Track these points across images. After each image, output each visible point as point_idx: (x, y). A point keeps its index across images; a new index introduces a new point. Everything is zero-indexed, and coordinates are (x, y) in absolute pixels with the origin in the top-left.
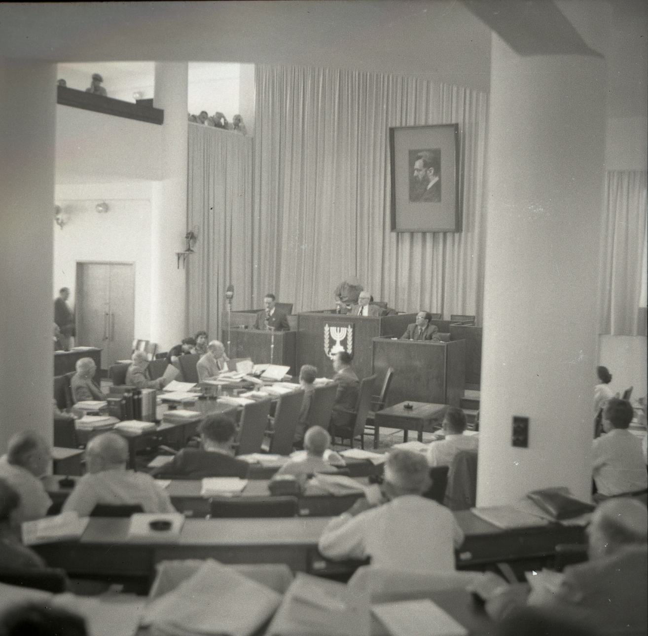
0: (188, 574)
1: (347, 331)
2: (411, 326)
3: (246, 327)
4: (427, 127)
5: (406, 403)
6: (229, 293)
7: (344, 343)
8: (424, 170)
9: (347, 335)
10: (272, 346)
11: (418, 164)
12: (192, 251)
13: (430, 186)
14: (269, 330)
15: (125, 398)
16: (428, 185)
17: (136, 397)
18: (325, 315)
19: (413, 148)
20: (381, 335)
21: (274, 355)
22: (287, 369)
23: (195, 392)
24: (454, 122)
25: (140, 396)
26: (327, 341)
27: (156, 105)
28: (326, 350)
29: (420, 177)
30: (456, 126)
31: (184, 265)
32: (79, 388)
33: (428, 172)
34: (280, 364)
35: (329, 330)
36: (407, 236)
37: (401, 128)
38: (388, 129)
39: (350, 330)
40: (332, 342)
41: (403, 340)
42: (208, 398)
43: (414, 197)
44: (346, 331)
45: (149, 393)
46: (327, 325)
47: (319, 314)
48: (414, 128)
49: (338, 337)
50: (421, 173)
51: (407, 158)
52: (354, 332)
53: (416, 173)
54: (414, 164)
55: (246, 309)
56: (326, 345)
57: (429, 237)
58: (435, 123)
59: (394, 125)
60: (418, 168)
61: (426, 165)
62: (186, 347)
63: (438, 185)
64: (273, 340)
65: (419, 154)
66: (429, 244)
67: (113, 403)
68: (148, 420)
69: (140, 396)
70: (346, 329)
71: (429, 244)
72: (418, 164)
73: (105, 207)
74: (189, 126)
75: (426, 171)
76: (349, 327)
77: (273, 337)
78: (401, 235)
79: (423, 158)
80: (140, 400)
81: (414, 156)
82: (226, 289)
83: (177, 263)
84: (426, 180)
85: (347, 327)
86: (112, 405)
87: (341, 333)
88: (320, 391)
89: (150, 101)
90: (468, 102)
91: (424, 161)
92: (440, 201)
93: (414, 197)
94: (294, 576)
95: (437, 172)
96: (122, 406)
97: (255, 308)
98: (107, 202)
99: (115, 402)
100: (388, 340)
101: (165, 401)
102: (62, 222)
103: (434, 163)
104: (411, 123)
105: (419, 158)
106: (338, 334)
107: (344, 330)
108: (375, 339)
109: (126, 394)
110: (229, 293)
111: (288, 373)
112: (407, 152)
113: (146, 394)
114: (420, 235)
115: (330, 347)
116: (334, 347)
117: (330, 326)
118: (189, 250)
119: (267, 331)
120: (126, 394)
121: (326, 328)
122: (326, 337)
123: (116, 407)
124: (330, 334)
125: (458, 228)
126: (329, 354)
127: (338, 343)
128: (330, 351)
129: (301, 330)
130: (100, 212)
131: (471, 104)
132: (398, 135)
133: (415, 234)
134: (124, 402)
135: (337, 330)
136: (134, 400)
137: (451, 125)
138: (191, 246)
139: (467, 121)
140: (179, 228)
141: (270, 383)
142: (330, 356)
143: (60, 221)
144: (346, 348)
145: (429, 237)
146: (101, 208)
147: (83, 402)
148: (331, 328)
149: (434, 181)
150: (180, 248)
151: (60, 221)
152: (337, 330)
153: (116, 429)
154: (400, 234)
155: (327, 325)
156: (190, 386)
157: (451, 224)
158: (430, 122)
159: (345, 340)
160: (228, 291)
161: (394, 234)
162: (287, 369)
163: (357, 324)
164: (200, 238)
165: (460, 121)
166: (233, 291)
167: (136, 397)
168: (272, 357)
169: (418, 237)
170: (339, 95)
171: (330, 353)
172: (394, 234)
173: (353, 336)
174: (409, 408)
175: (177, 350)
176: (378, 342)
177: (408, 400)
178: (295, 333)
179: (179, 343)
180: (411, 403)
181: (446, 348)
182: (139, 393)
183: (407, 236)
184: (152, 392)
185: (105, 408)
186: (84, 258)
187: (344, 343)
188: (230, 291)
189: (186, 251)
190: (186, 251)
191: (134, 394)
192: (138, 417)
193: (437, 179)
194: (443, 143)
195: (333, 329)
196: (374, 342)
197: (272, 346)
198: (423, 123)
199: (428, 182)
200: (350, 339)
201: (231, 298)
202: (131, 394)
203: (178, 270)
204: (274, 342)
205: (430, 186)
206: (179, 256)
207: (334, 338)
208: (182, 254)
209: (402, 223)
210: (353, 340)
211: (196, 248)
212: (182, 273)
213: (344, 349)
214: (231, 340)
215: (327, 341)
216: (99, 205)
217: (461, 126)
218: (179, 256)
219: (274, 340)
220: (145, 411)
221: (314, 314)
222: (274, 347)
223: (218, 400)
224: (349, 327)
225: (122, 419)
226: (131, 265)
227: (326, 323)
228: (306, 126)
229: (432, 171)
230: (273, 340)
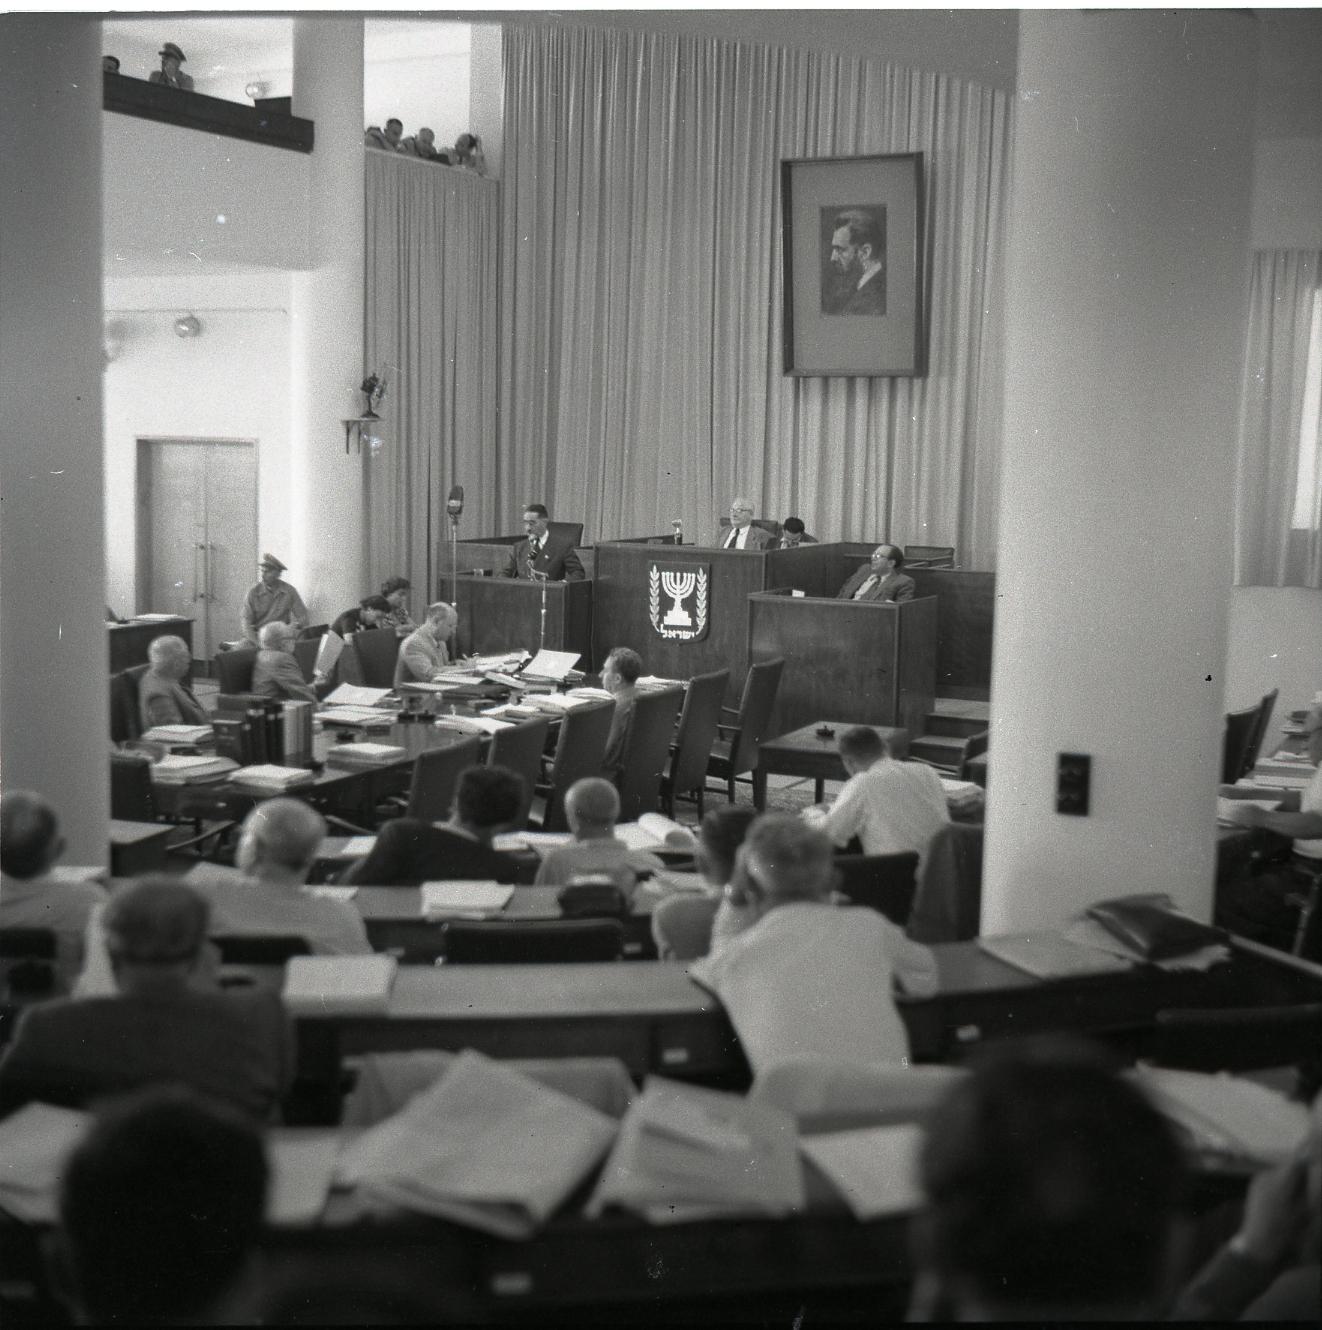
0: (423, 1083)
1: (697, 580)
3: (488, 573)
4: (858, 159)
5: (821, 725)
6: (454, 503)
7: (689, 604)
8: (851, 249)
9: (696, 588)
10: (543, 611)
11: (840, 236)
12: (376, 416)
13: (862, 282)
14: (536, 578)
15: (250, 719)
16: (859, 278)
17: (271, 717)
18: (650, 546)
19: (827, 203)
20: (765, 589)
21: (545, 631)
22: (575, 657)
23: (390, 706)
24: (913, 149)
25: (280, 715)
26: (654, 601)
27: (296, 111)
28: (654, 619)
30: (918, 157)
31: (359, 444)
32: (154, 698)
33: (860, 253)
34: (559, 650)
35: (660, 579)
36: (815, 385)
37: (806, 162)
38: (779, 165)
39: (703, 578)
40: (666, 603)
42: (416, 719)
43: (832, 304)
44: (693, 583)
45: (298, 709)
46: (655, 568)
47: (640, 546)
48: (832, 161)
49: (678, 592)
50: (845, 254)
51: (817, 221)
52: (710, 582)
53: (835, 255)
55: (484, 536)
56: (654, 609)
57: (861, 385)
58: (876, 151)
59: (790, 156)
60: (840, 244)
61: (856, 239)
62: (371, 614)
63: (879, 280)
64: (544, 601)
66: (861, 402)
67: (225, 730)
68: (296, 764)
69: (280, 715)
70: (694, 575)
71: (861, 402)
72: (840, 236)
73: (193, 326)
74: (368, 155)
75: (856, 252)
76: (701, 571)
77: (544, 592)
78: (805, 384)
79: (851, 224)
80: (279, 723)
81: (831, 218)
82: (447, 494)
83: (344, 441)
84: (856, 270)
85: (697, 573)
86: (224, 734)
87: (683, 584)
88: (647, 705)
89: (287, 100)
90: (941, 109)
91: (852, 230)
92: (883, 312)
93: (832, 304)
94: (639, 1083)
95: (879, 252)
96: (243, 735)
97: (504, 534)
98: (196, 315)
99: (229, 726)
100: (781, 598)
101: (329, 724)
103: (873, 233)
104: (826, 151)
105: (844, 222)
106: (678, 587)
107: (689, 577)
108: (755, 596)
109: (252, 712)
111: (575, 667)
112: (817, 211)
113: (291, 711)
114: (842, 381)
115: (662, 613)
116: (669, 612)
117: (659, 570)
118: (369, 414)
119: (532, 582)
120: (252, 712)
121: (654, 575)
122: (654, 591)
123: (232, 738)
124: (661, 586)
125: (921, 368)
126: (659, 627)
128: (661, 621)
130: (183, 335)
131: (948, 111)
132: (797, 174)
133: (832, 381)
134: (247, 727)
135: (675, 577)
136: (268, 723)
137: (907, 156)
138: (373, 405)
139: (940, 147)
140: (349, 368)
141: (543, 688)
142: (662, 631)
144: (693, 615)
145: (861, 385)
146: (185, 328)
147: (164, 728)
148: (663, 573)
149: (871, 270)
150: (348, 410)
152: (675, 577)
153: (232, 782)
154: (801, 380)
155: (655, 568)
156: (378, 694)
157: (909, 364)
158: (865, 151)
159: (694, 596)
160: (451, 498)
161: (790, 380)
162: (575, 657)
163: (715, 564)
164: (392, 388)
165: (927, 148)
167: (271, 717)
169: (839, 387)
170: (678, 92)
171: (662, 626)
172: (790, 380)
173: (709, 589)
174: (826, 735)
175: (351, 619)
176: (759, 603)
177: (824, 720)
179: (356, 605)
180: (831, 726)
181: (897, 612)
182: (279, 709)
183: (815, 385)
184: (305, 706)
185: (209, 738)
186: (152, 432)
187: (689, 604)
188: (456, 499)
189: (364, 416)
190: (364, 416)
191: (267, 712)
192: (276, 758)
193: (877, 267)
194: (890, 192)
195: (667, 576)
197: (543, 611)
198: (850, 151)
199: (860, 273)
200: (702, 595)
201: (460, 511)
202: (261, 712)
204: (546, 603)
205: (862, 282)
207: (671, 595)
208: (355, 422)
209: (805, 360)
210: (709, 598)
211: (386, 407)
212: (355, 461)
215: (654, 601)
216: (181, 322)
217: (928, 159)
218: (348, 426)
219: (547, 597)
220: (289, 747)
221: (624, 545)
222: (547, 614)
223: (438, 723)
224: (701, 571)
225: (244, 762)
226: (249, 445)
227: (653, 564)
228: (608, 163)
229: (869, 252)
230: (544, 601)
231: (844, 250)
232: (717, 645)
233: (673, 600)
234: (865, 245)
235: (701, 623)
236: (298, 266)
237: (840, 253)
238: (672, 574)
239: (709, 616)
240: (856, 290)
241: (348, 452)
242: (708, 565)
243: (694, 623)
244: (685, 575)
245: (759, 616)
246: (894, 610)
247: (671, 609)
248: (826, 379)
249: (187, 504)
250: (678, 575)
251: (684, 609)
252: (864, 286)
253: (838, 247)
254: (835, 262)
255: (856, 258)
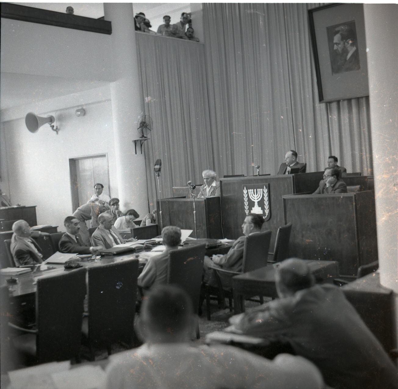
1: (263, 192)
2: (322, 182)
6: (157, 167)
8: (342, 43)
9: (263, 196)
10: (194, 212)
11: (337, 38)
16: (347, 55)
20: (294, 193)
21: (196, 221)
26: (246, 203)
27: (106, 19)
29: (340, 50)
33: (346, 44)
35: (248, 193)
36: (334, 106)
39: (266, 191)
40: (251, 204)
41: (315, 195)
43: (336, 69)
49: (256, 198)
50: (340, 46)
52: (269, 192)
53: (335, 47)
54: (333, 40)
56: (246, 207)
57: (353, 102)
60: (338, 42)
61: (344, 38)
63: (356, 55)
65: (337, 29)
66: (354, 110)
70: (262, 190)
71: (354, 110)
72: (337, 38)
73: (83, 112)
75: (344, 43)
77: (194, 203)
79: (340, 32)
81: (331, 32)
85: (263, 188)
89: (103, 17)
91: (341, 34)
92: (359, 68)
93: (336, 69)
98: (84, 107)
102: (57, 128)
106: (256, 196)
107: (260, 191)
110: (157, 167)
111: (190, 236)
114: (346, 103)
115: (250, 209)
116: (253, 208)
117: (247, 189)
118: (143, 136)
121: (245, 191)
122: (246, 199)
124: (248, 196)
127: (256, 204)
128: (250, 212)
129: (224, 195)
130: (79, 116)
132: (316, 15)
133: (341, 103)
143: (55, 128)
144: (263, 209)
145: (353, 102)
148: (249, 190)
149: (352, 51)
150: (137, 137)
151: (55, 128)
154: (328, 104)
159: (263, 199)
161: (323, 105)
166: (160, 165)
168: (195, 222)
173: (269, 196)
176: (288, 199)
178: (218, 198)
181: (354, 198)
183: (334, 106)
187: (261, 204)
189: (140, 138)
196: (284, 200)
197: (194, 212)
200: (266, 199)
201: (159, 170)
203: (136, 155)
206: (135, 142)
207: (253, 200)
208: (137, 140)
212: (140, 158)
213: (262, 209)
214: (161, 211)
215: (246, 203)
216: (78, 111)
218: (135, 142)
219: (195, 204)
226: (103, 156)
231: (339, 44)
232: (275, 222)
233: (254, 202)
234: (348, 40)
235: (267, 212)
236: (111, 81)
237: (338, 46)
238: (253, 190)
239: (270, 208)
240: (346, 60)
241: (136, 153)
242: (267, 184)
243: (264, 212)
244: (258, 190)
245: (289, 206)
246: (352, 197)
247: (254, 207)
248: (338, 102)
249: (89, 183)
250: (255, 190)
251: (259, 206)
252: (349, 58)
253: (336, 44)
254: (336, 50)
255: (344, 47)
